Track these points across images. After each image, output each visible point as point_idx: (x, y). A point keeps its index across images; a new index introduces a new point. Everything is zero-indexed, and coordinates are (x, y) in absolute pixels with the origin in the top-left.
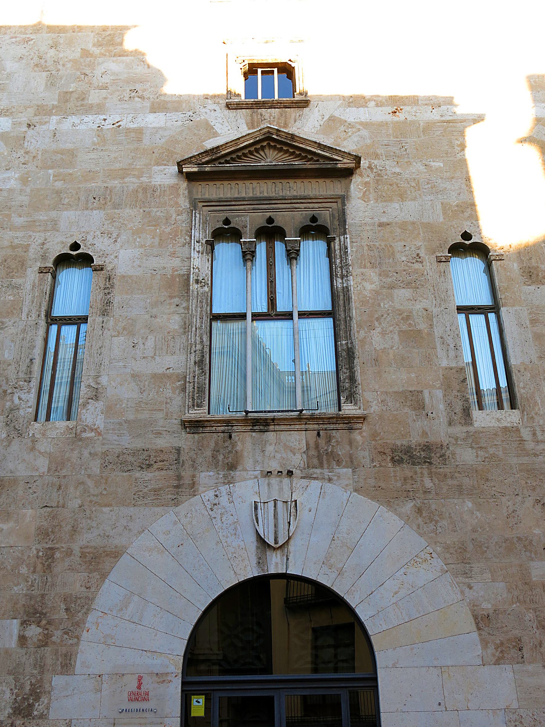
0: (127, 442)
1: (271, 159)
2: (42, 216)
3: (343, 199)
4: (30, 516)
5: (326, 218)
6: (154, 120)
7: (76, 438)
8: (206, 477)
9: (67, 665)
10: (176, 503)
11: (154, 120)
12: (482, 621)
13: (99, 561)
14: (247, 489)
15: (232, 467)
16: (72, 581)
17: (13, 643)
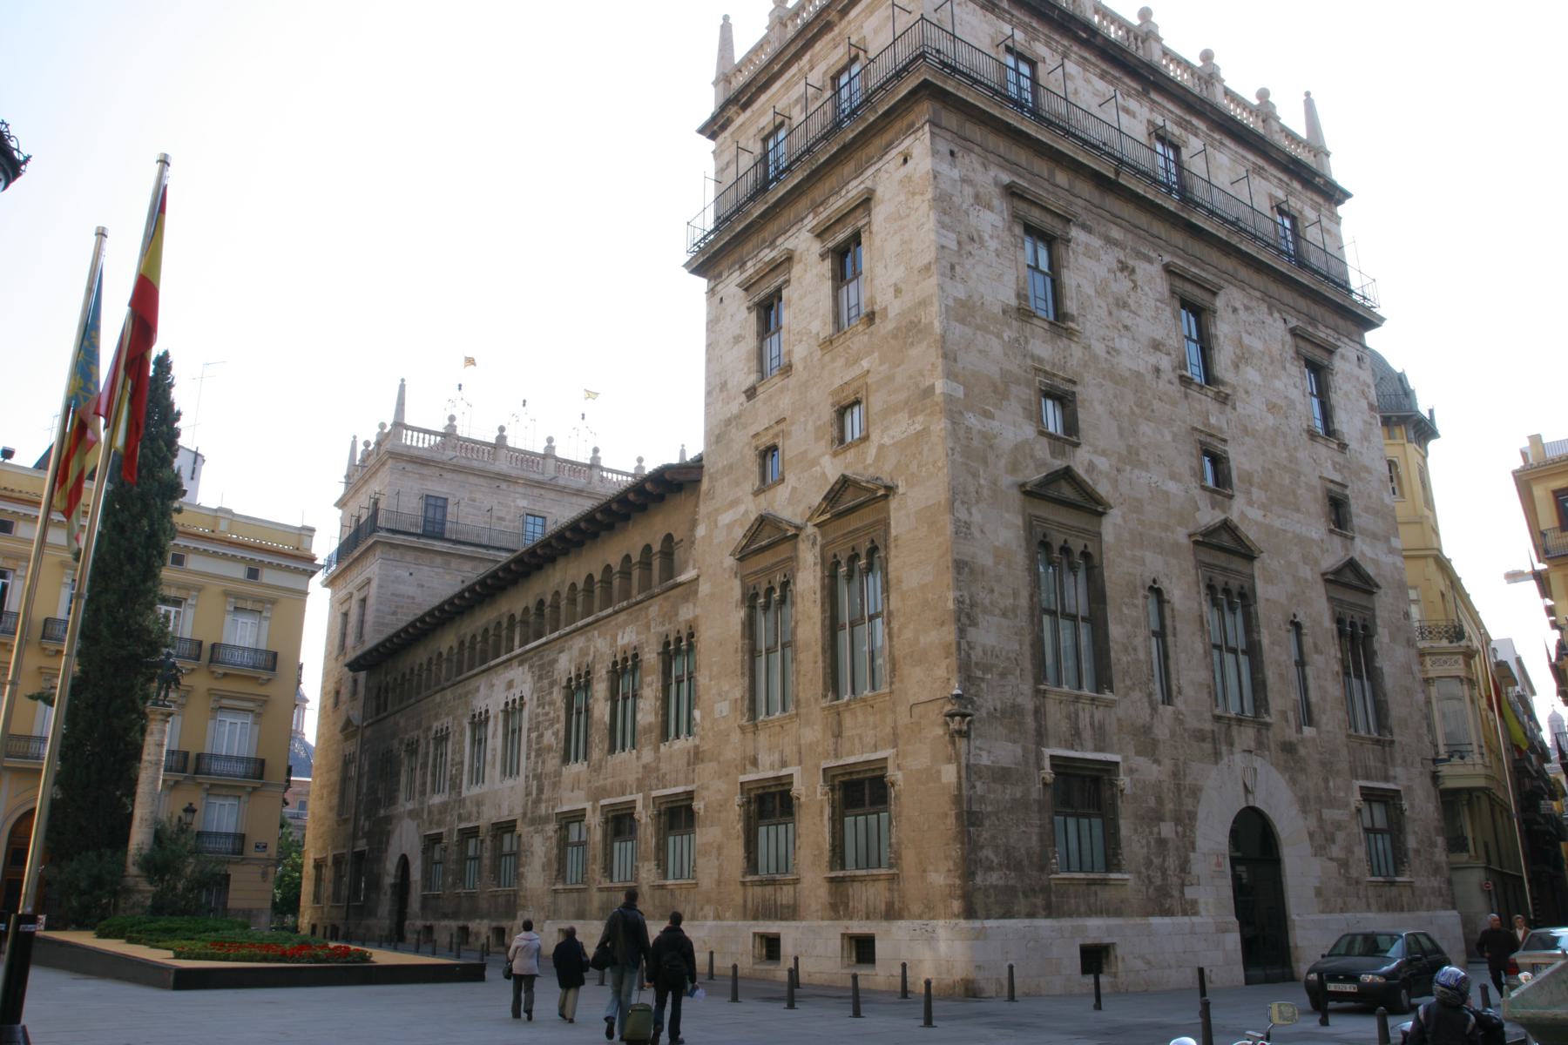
0: (1192, 723)
1: (1226, 540)
2: (1138, 553)
3: (1252, 577)
4: (1168, 763)
5: (1246, 590)
6: (1172, 486)
7: (1179, 719)
8: (1224, 749)
9: (1194, 849)
10: (1216, 763)
11: (1172, 486)
12: (1311, 835)
13: (1195, 792)
14: (1239, 759)
15: (1231, 744)
16: (1188, 803)
17: (1173, 835)
